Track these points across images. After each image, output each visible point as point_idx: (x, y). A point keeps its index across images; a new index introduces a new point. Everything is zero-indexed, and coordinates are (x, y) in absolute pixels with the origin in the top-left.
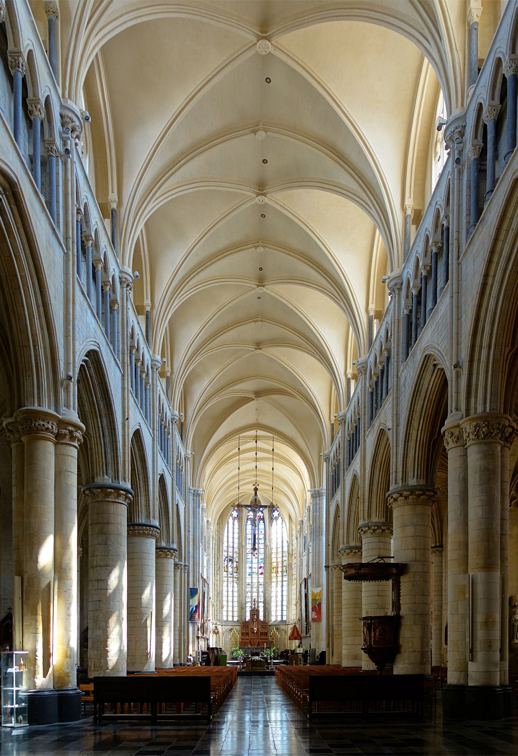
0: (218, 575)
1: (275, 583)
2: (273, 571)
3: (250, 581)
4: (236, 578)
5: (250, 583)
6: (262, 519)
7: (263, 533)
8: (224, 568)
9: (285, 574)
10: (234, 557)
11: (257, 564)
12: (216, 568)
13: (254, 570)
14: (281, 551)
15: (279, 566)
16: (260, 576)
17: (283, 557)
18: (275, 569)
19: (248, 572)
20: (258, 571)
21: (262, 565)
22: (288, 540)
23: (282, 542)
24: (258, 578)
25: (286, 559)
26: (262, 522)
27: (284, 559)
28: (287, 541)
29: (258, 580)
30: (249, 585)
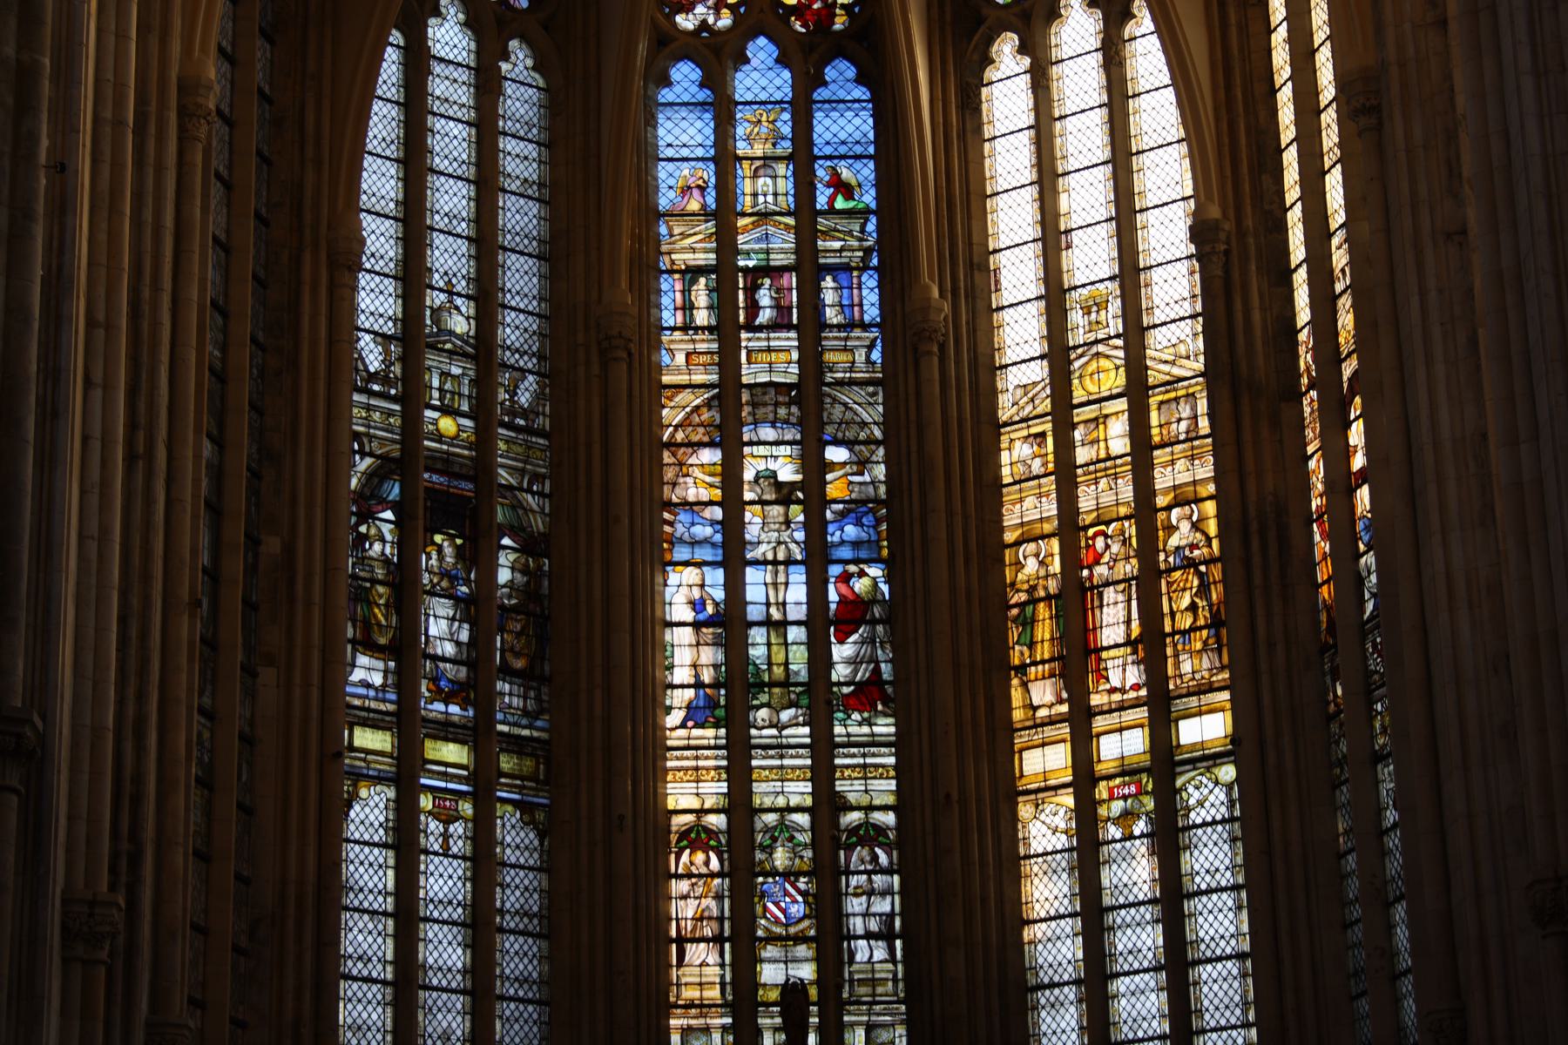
0: (268, 676)
1: (1068, 800)
2: (1018, 655)
3: (714, 790)
4: (515, 745)
5: (717, 821)
6: (840, 47)
7: (869, 198)
8: (361, 596)
9: (1189, 666)
10: (504, 476)
11: (798, 576)
12: (235, 566)
13: (758, 645)
14: (1114, 380)
15: (1101, 571)
16: (849, 727)
17: (1142, 447)
18: (1044, 631)
19: (682, 675)
20: (820, 659)
21: (871, 579)
22: (1214, 212)
23: (1130, 273)
24: (823, 749)
25: (1205, 470)
26: (840, 74)
27: (1163, 479)
28: (1200, 232)
29: (823, 774)
30: (697, 838)
